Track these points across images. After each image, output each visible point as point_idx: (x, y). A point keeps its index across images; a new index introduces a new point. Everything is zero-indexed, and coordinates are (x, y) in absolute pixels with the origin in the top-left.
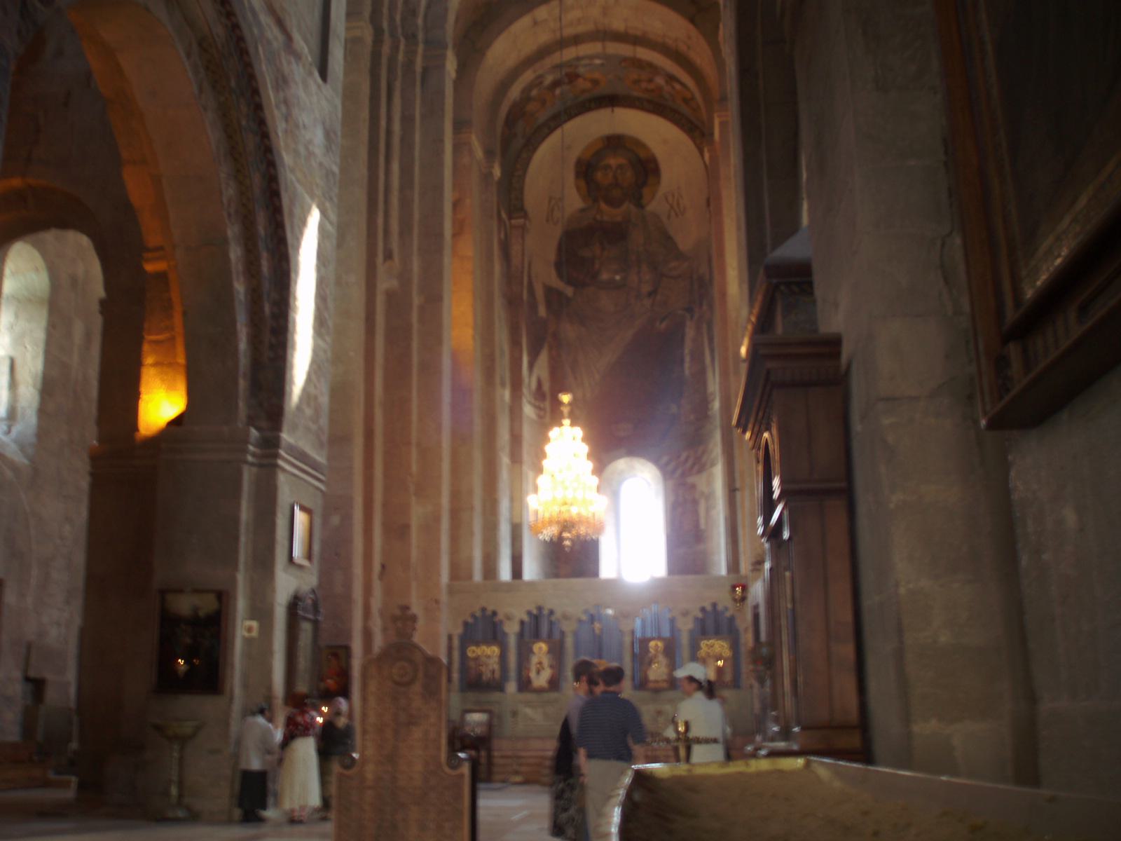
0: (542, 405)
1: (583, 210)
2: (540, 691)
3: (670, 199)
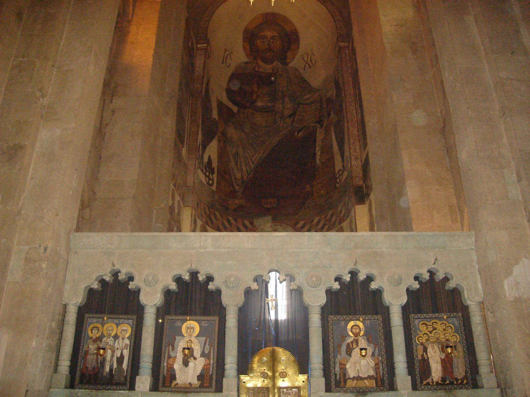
0: (211, 177)
1: (246, 63)
2: (187, 389)
3: (305, 59)
